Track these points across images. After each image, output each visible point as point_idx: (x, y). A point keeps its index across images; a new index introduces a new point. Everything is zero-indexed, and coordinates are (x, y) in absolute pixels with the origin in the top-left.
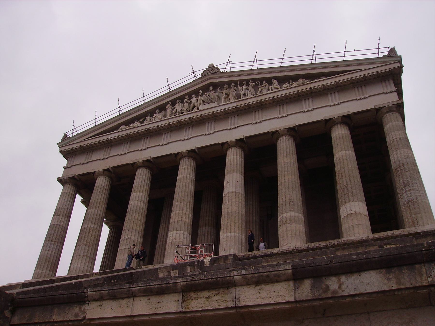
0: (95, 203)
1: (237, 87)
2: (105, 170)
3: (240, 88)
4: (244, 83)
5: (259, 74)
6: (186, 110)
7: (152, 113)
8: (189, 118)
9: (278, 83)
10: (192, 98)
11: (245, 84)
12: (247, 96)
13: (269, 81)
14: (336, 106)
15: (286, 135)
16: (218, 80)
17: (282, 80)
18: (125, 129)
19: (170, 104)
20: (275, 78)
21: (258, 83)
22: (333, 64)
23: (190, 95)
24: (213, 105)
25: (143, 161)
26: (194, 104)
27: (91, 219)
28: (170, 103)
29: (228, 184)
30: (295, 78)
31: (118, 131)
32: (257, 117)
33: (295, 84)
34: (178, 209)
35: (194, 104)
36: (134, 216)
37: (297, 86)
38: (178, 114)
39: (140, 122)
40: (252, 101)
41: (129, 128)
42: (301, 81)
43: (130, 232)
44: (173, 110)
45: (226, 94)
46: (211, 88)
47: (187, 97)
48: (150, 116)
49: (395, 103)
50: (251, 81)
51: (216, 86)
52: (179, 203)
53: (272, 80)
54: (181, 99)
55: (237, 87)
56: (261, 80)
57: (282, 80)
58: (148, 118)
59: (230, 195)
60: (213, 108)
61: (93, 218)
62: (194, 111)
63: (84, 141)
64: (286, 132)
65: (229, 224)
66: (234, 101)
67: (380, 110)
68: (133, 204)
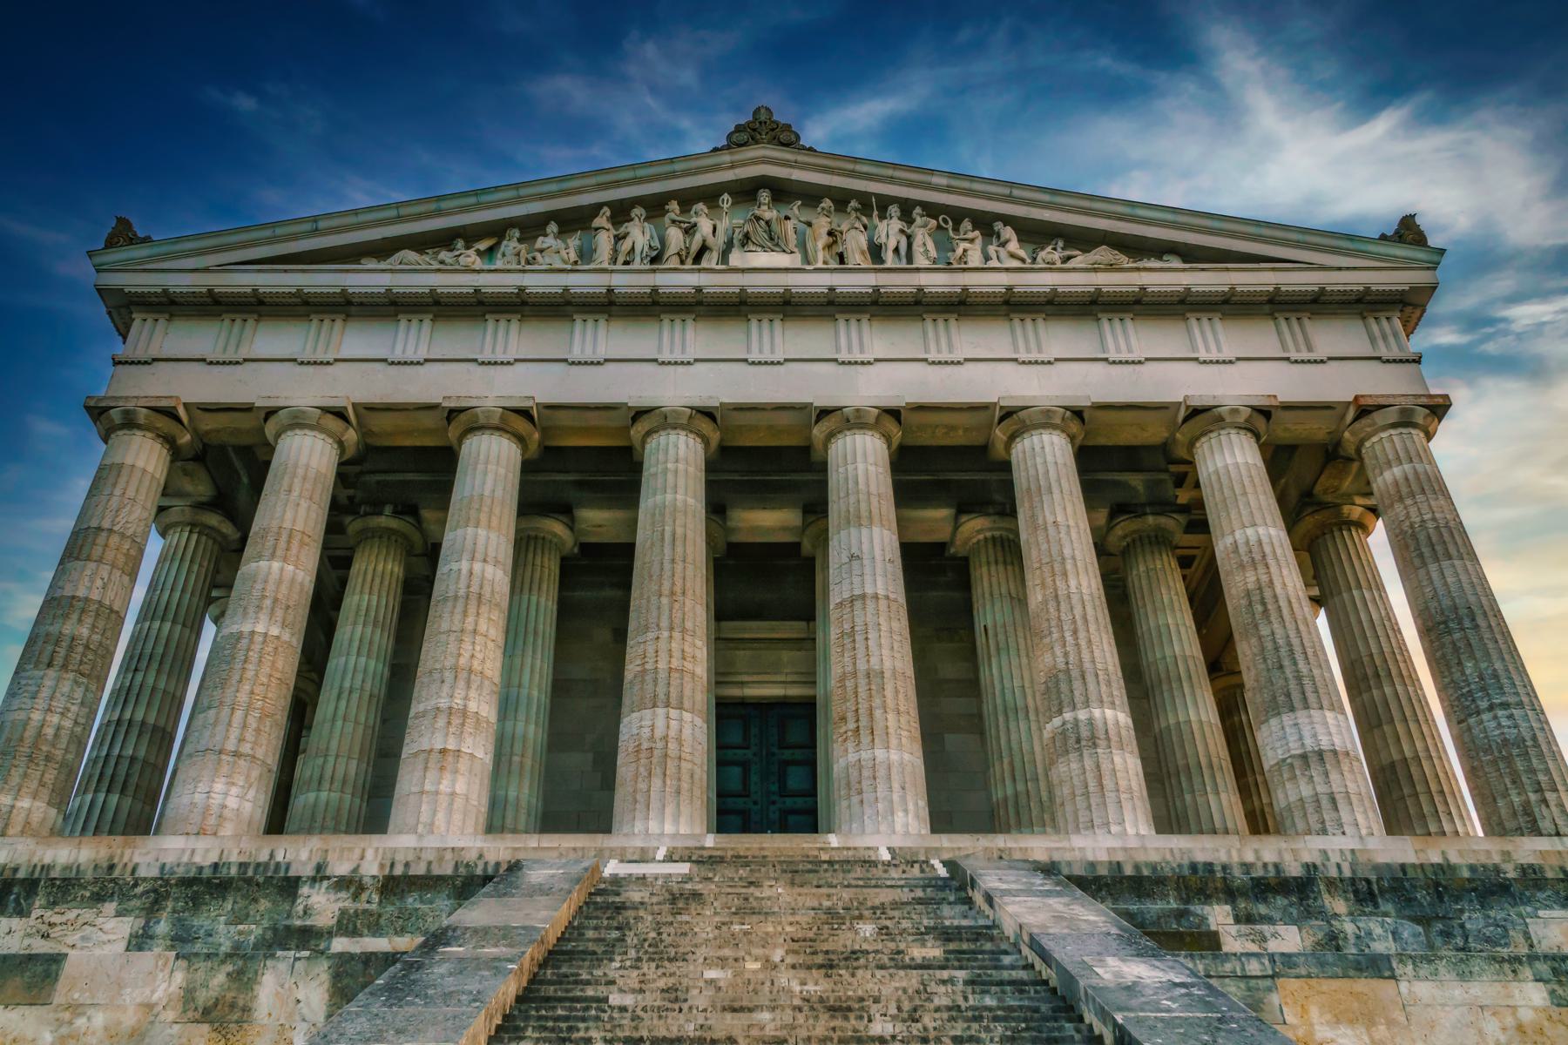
0: (284, 538)
1: (870, 216)
2: (326, 410)
3: (882, 227)
4: (894, 210)
5: (949, 192)
6: (678, 254)
7: (531, 228)
8: (694, 287)
9: (1020, 241)
10: (692, 212)
11: (899, 214)
12: (904, 260)
13: (985, 224)
14: (1222, 367)
15: (1054, 427)
16: (797, 175)
18: (418, 267)
19: (608, 213)
20: (1008, 220)
21: (944, 220)
22: (1217, 224)
23: (687, 199)
25: (503, 408)
26: (704, 241)
27: (268, 602)
28: (607, 211)
29: (855, 564)
30: (1082, 240)
31: (383, 266)
32: (943, 341)
33: (1080, 260)
34: (664, 623)
35: (704, 241)
36: (470, 619)
37: (1095, 270)
38: (638, 259)
39: (479, 253)
40: (938, 282)
41: (436, 266)
42: (1103, 254)
43: (461, 683)
44: (619, 239)
45: (830, 233)
46: (764, 196)
47: (674, 206)
48: (520, 240)
49: (1424, 401)
50: (918, 210)
51: (782, 192)
52: (665, 600)
53: (998, 226)
54: (655, 207)
55: (870, 216)
56: (957, 216)
57: (1035, 234)
58: (511, 245)
59: (870, 604)
60: (787, 270)
61: (276, 600)
62: (704, 264)
63: (222, 268)
64: (1058, 421)
65: (878, 713)
66: (863, 266)
67: (1370, 412)
68: (464, 571)
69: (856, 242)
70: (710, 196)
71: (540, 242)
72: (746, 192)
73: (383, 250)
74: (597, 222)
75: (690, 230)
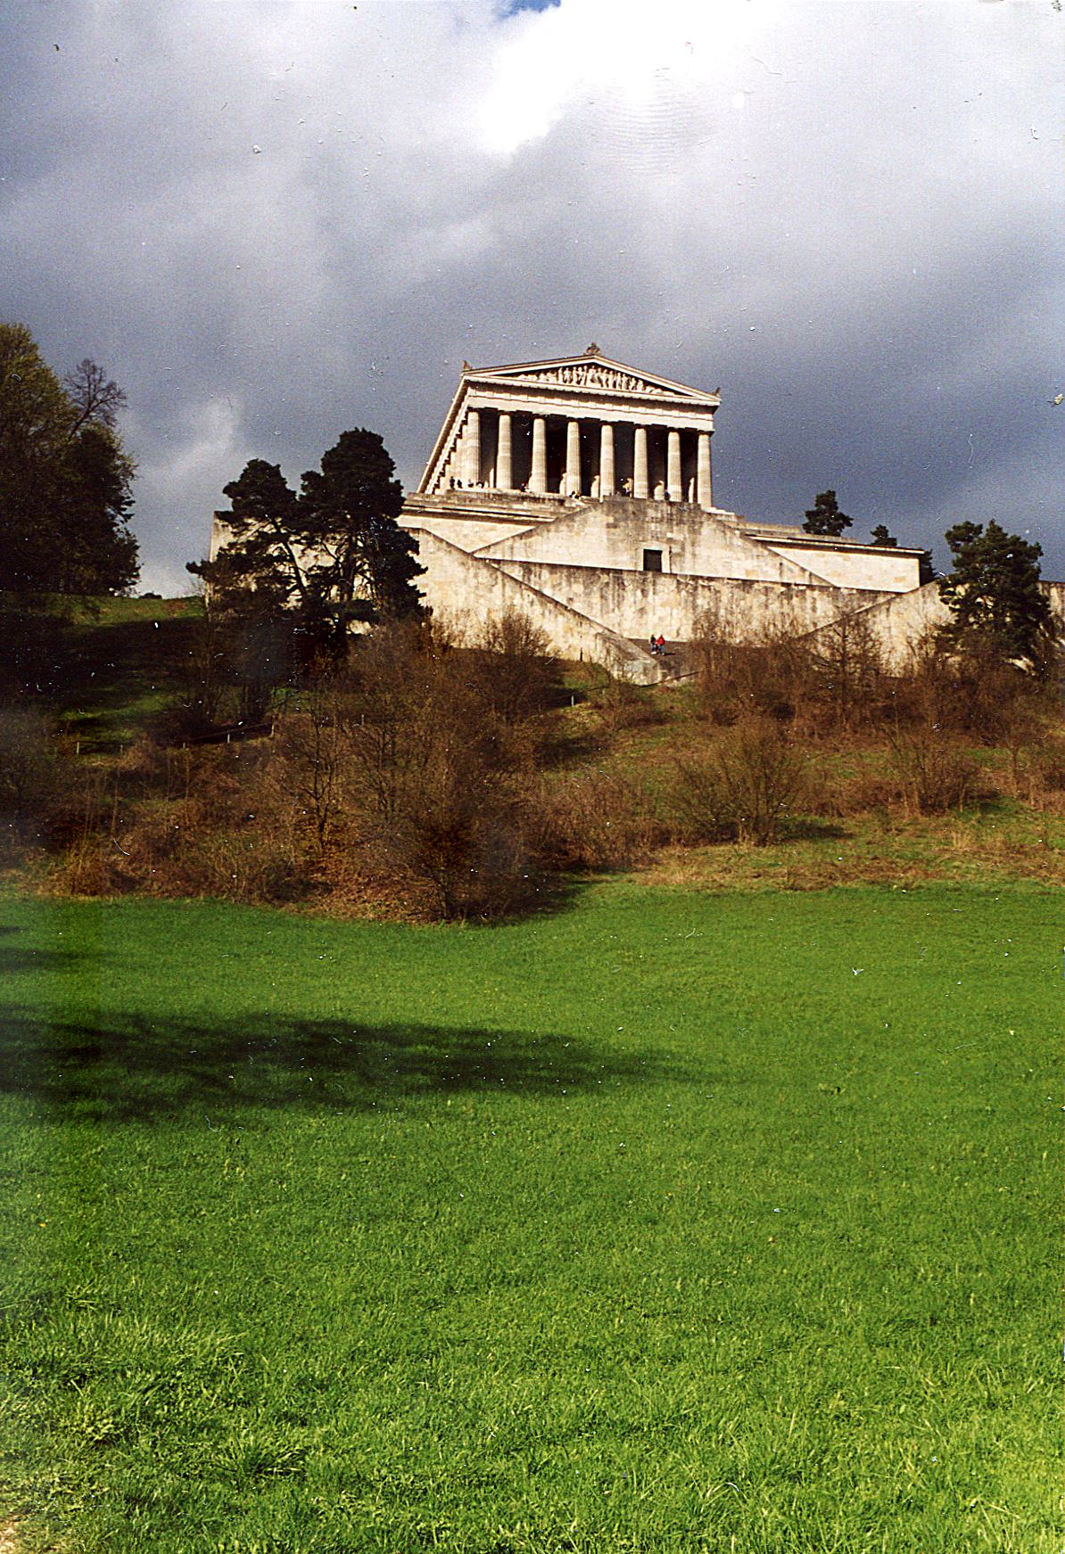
17: (646, 383)
24: (599, 386)
40: (627, 395)
42: (659, 390)
54: (571, 368)
56: (632, 377)
69: (610, 383)
70: (582, 366)
71: (549, 374)
72: (589, 366)
73: (518, 374)
74: (560, 371)
75: (578, 375)
